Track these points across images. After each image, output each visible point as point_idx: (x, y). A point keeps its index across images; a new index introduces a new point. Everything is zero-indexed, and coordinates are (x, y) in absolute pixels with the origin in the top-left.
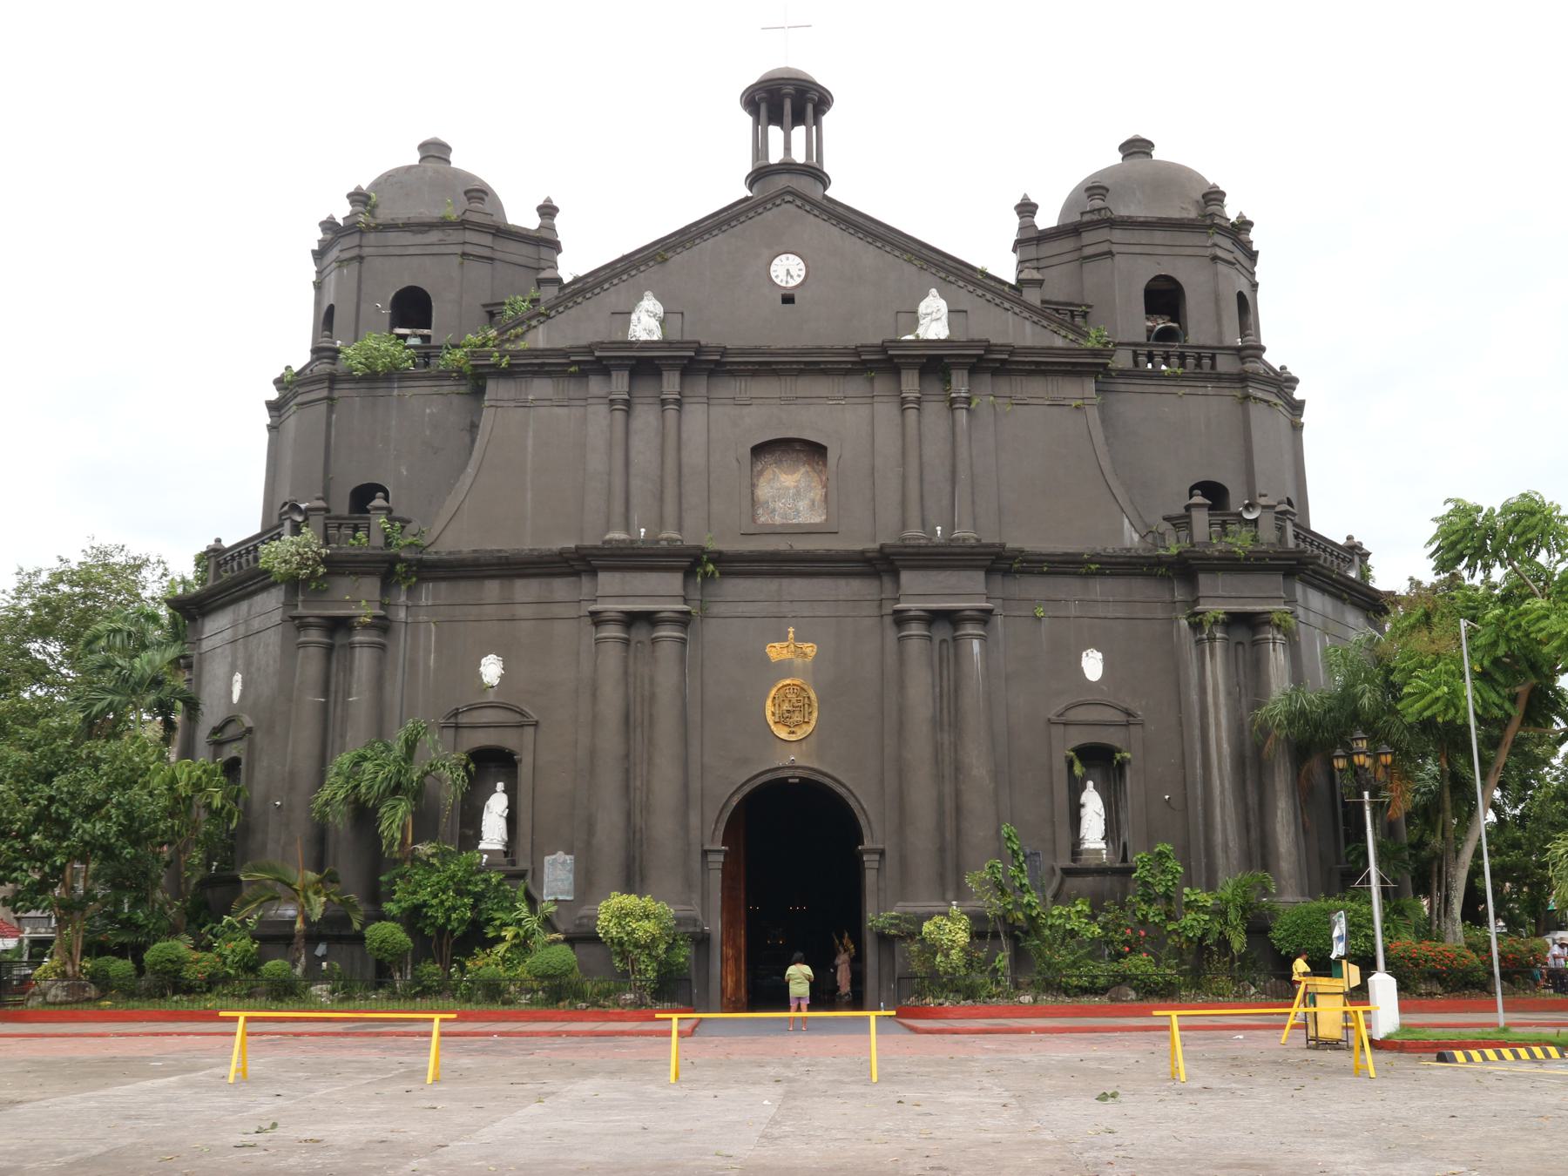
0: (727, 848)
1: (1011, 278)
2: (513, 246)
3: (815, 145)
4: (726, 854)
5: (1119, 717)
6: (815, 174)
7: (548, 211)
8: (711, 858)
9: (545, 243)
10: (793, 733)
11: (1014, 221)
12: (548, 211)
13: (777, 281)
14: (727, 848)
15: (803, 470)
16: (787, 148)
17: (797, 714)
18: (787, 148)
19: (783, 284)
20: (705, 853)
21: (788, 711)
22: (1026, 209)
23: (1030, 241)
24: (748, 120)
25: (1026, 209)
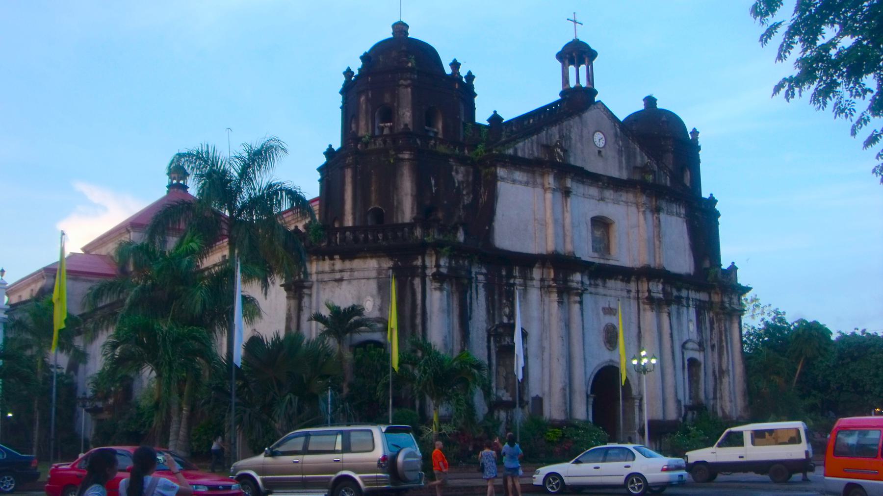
6: (590, 92)
13: (596, 143)
15: (601, 230)
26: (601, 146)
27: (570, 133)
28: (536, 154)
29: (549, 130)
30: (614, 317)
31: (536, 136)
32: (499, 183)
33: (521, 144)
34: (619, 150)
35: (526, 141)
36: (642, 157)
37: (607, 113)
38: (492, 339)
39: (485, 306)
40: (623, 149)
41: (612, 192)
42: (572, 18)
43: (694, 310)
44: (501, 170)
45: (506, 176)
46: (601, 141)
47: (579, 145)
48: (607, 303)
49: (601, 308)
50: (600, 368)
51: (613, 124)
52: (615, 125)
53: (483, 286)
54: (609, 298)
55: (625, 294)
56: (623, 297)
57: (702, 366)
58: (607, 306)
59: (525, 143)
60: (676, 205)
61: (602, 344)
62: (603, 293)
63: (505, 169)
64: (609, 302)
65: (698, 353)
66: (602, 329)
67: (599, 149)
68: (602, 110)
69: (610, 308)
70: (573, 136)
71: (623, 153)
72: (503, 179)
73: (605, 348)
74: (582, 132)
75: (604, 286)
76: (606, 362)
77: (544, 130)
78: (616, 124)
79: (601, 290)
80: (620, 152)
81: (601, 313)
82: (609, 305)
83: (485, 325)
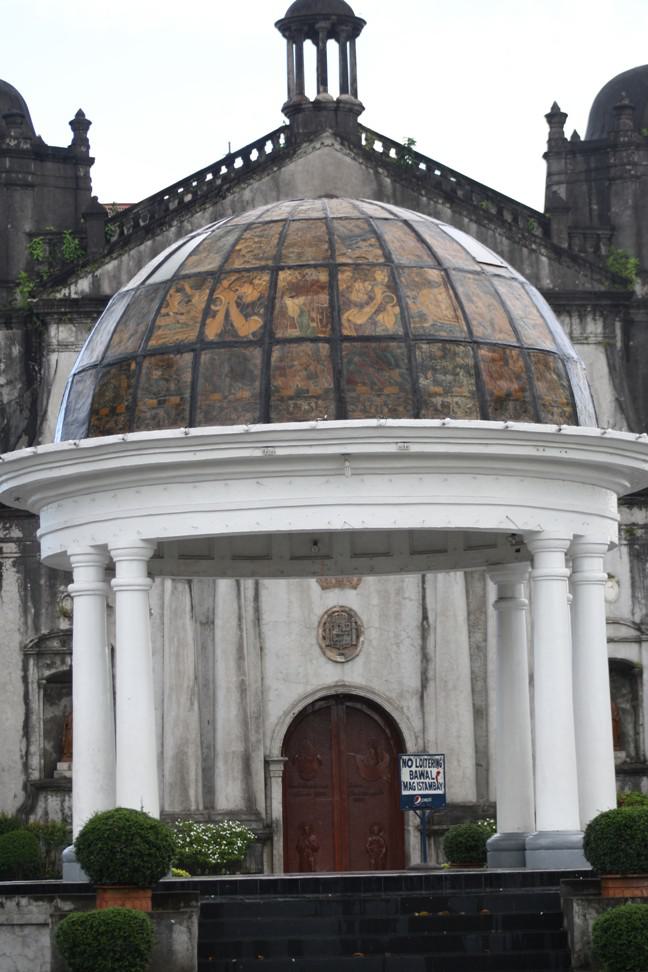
0: (286, 759)
1: (538, 204)
2: (50, 166)
3: (348, 82)
4: (286, 764)
5: (633, 633)
7: (80, 124)
8: (273, 767)
9: (77, 158)
10: (343, 654)
11: (544, 129)
12: (80, 124)
14: (286, 759)
16: (322, 80)
17: (345, 637)
18: (322, 80)
20: (267, 763)
21: (338, 635)
22: (556, 117)
23: (559, 149)
24: (280, 42)
25: (556, 117)
29: (185, 223)
30: (354, 592)
31: (149, 243)
32: (54, 357)
33: (110, 266)
35: (125, 258)
37: (350, 149)
38: (31, 662)
39: (19, 602)
44: (61, 329)
45: (72, 339)
51: (371, 171)
52: (377, 173)
53: (14, 564)
59: (121, 261)
60: (571, 316)
61: (317, 651)
63: (71, 326)
65: (635, 646)
66: (315, 620)
68: (338, 146)
72: (64, 346)
73: (323, 659)
76: (329, 687)
77: (171, 226)
78: (380, 170)
83: (17, 638)
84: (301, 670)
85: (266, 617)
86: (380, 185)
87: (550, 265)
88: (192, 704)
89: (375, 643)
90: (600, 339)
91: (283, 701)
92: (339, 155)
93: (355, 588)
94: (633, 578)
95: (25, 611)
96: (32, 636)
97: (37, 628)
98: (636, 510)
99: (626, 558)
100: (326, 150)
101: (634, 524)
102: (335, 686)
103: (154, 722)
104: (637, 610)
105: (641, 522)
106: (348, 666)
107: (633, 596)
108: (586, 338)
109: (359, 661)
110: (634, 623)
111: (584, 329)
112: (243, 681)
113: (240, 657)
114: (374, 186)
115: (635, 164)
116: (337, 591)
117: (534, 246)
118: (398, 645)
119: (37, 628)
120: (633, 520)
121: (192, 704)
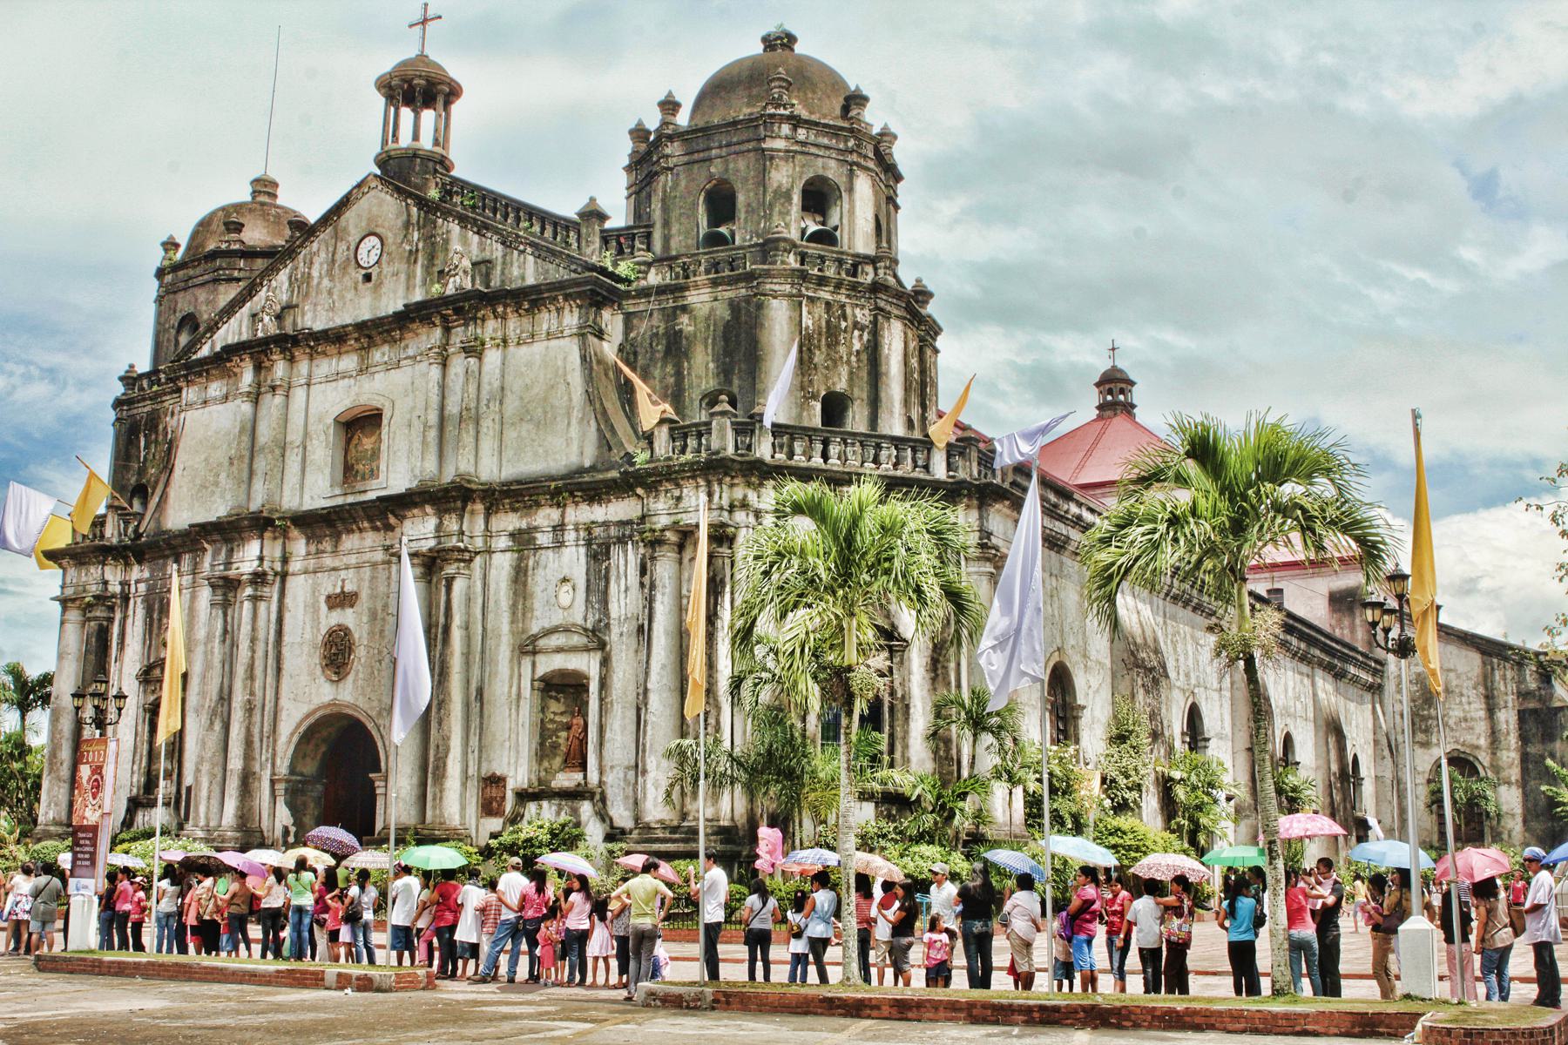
13: (361, 263)
19: (366, 265)
20: (273, 782)
26: (372, 263)
27: (310, 268)
28: (244, 337)
30: (351, 610)
34: (411, 251)
35: (232, 320)
36: (465, 241)
40: (421, 245)
41: (386, 348)
42: (430, 14)
43: (582, 550)
46: (374, 252)
47: (326, 282)
48: (340, 583)
49: (322, 599)
50: (312, 720)
53: (143, 601)
54: (343, 574)
55: (379, 556)
56: (374, 565)
57: (594, 687)
58: (338, 590)
61: (318, 671)
62: (332, 565)
64: (343, 581)
67: (363, 272)
68: (380, 187)
69: (343, 592)
70: (315, 274)
71: (420, 255)
73: (323, 679)
74: (334, 254)
75: (335, 552)
79: (328, 561)
80: (412, 256)
81: (324, 607)
82: (342, 588)
84: (307, 690)
85: (287, 639)
86: (409, 215)
87: (536, 263)
88: (212, 723)
89: (363, 660)
90: (575, 331)
91: (292, 719)
92: (383, 195)
93: (352, 606)
94: (588, 581)
95: (144, 643)
96: (146, 663)
97: (149, 658)
98: (596, 507)
99: (583, 560)
100: (372, 193)
101: (593, 522)
102: (329, 705)
103: (418, 755)
104: (590, 616)
105: (600, 519)
106: (341, 685)
107: (587, 600)
108: (562, 332)
109: (350, 678)
110: (586, 630)
111: (560, 323)
112: (249, 701)
113: (251, 676)
114: (404, 217)
115: (667, 156)
116: (339, 610)
117: (522, 247)
118: (380, 661)
119: (149, 658)
120: (593, 518)
121: (212, 723)
